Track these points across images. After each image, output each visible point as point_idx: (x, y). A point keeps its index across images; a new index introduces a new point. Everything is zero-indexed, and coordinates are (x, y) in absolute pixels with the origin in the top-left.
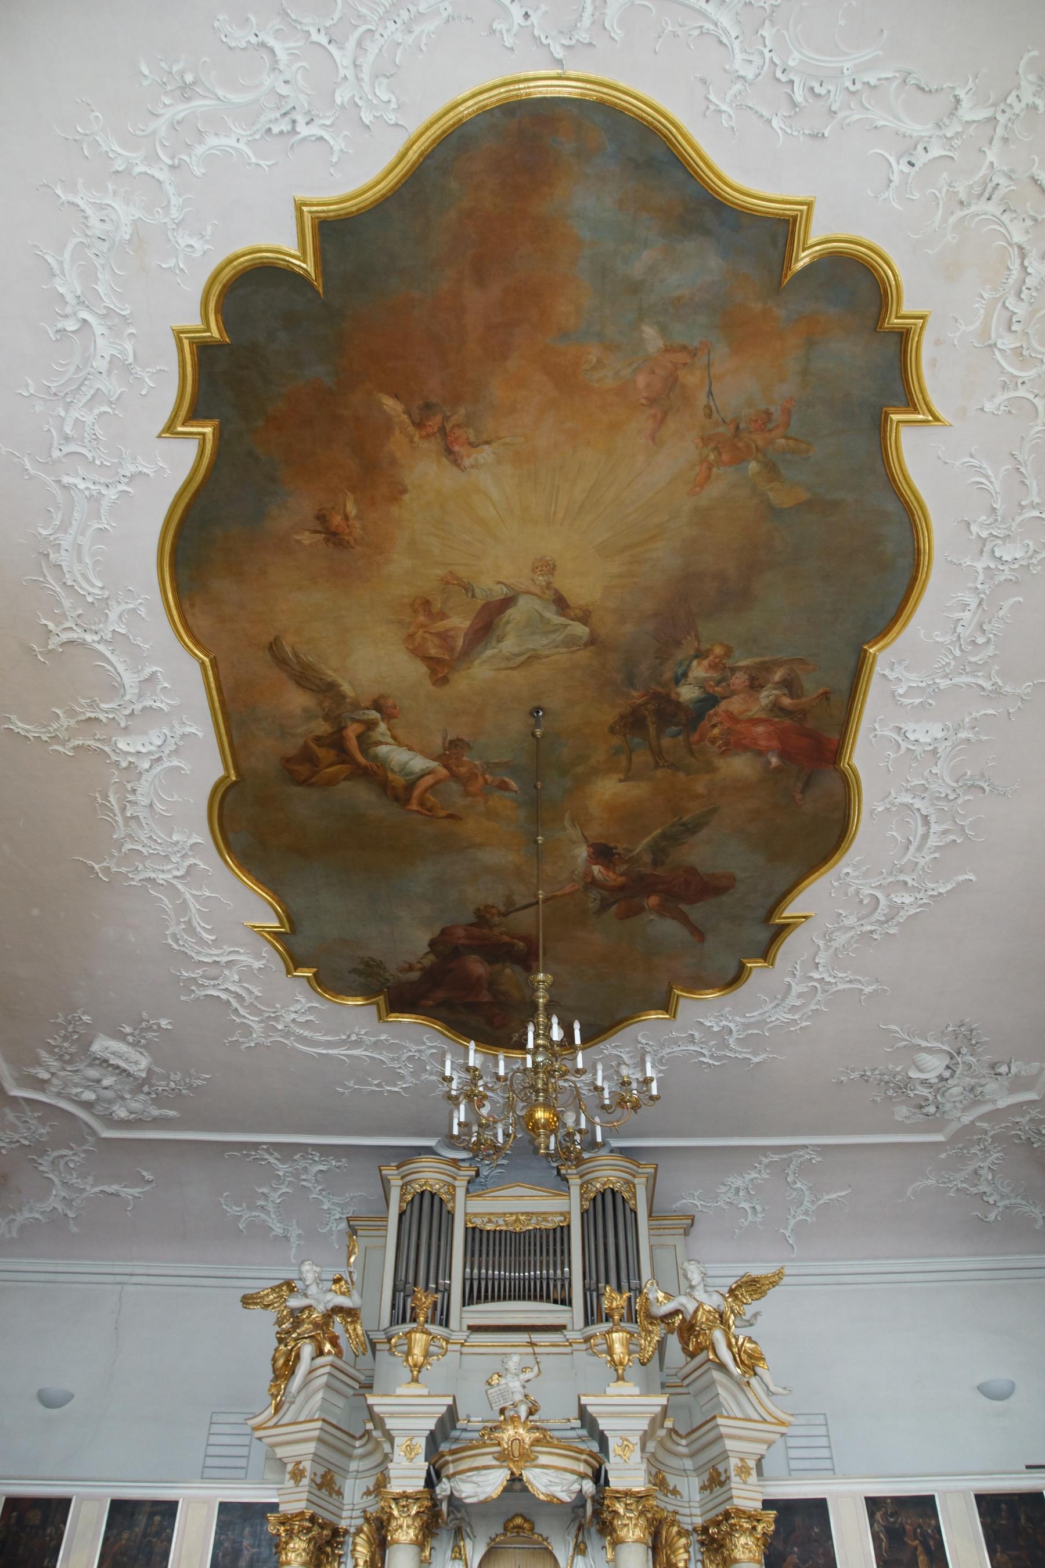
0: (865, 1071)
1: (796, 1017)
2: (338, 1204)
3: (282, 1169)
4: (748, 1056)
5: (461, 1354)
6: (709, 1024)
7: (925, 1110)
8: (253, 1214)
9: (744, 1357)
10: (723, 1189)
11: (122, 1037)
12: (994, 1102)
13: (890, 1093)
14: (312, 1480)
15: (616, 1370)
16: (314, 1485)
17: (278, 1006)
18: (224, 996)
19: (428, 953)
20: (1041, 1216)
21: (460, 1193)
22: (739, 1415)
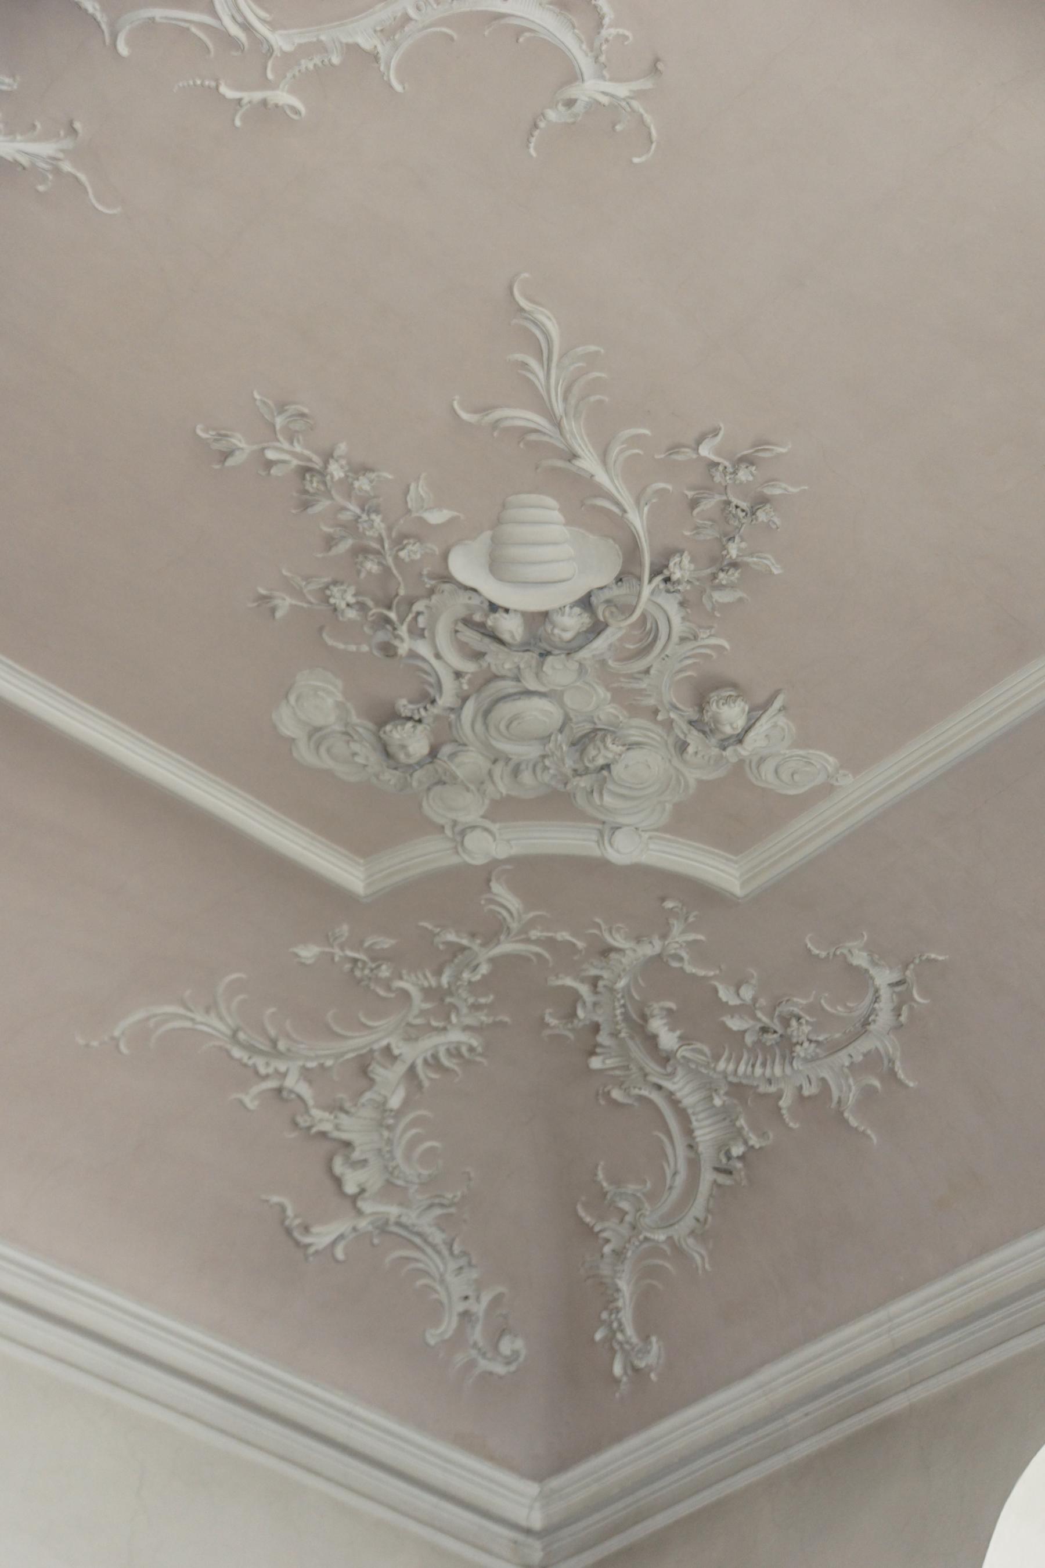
0: (328, 456)
1: (281, 41)
7: (396, 734)
12: (609, 829)
13: (343, 597)
20: (461, 1307)
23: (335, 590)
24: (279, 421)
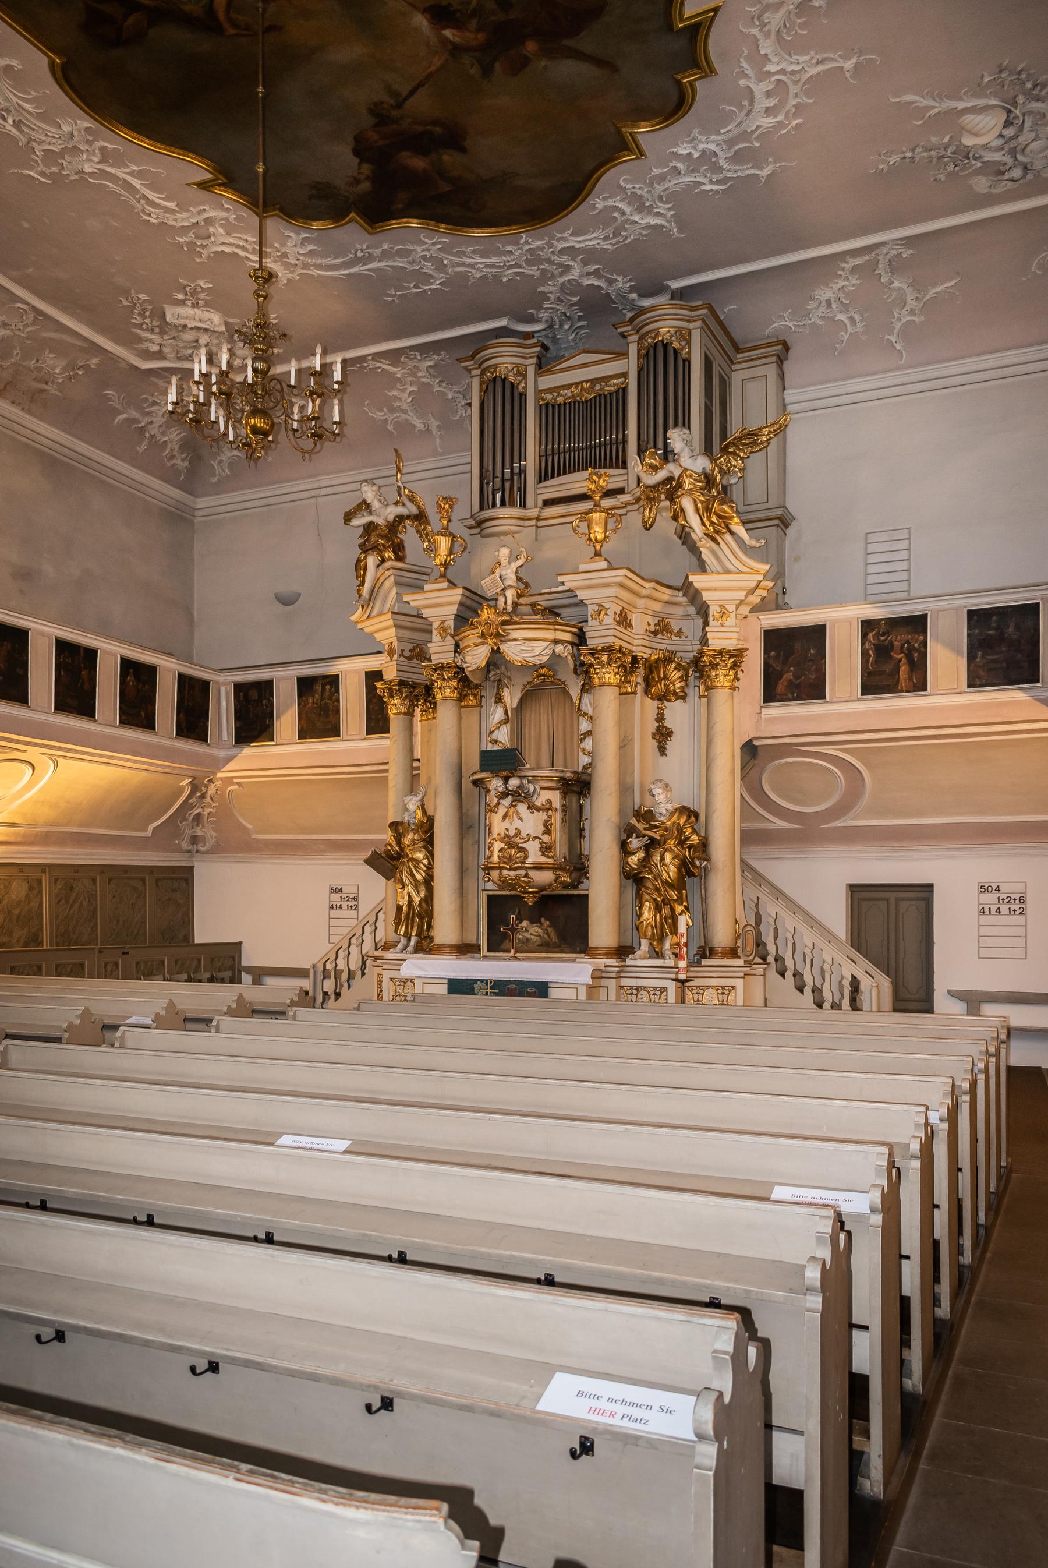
1: (779, 118)
2: (459, 392)
3: (398, 372)
4: (752, 172)
5: (537, 527)
6: (685, 152)
8: (395, 415)
9: (714, 519)
10: (812, 305)
11: (183, 303)
14: (400, 656)
15: (594, 546)
16: (402, 659)
17: (276, 245)
18: (227, 249)
19: (360, 164)
21: (531, 371)
22: (720, 569)
23: (947, 167)
24: (883, 157)
